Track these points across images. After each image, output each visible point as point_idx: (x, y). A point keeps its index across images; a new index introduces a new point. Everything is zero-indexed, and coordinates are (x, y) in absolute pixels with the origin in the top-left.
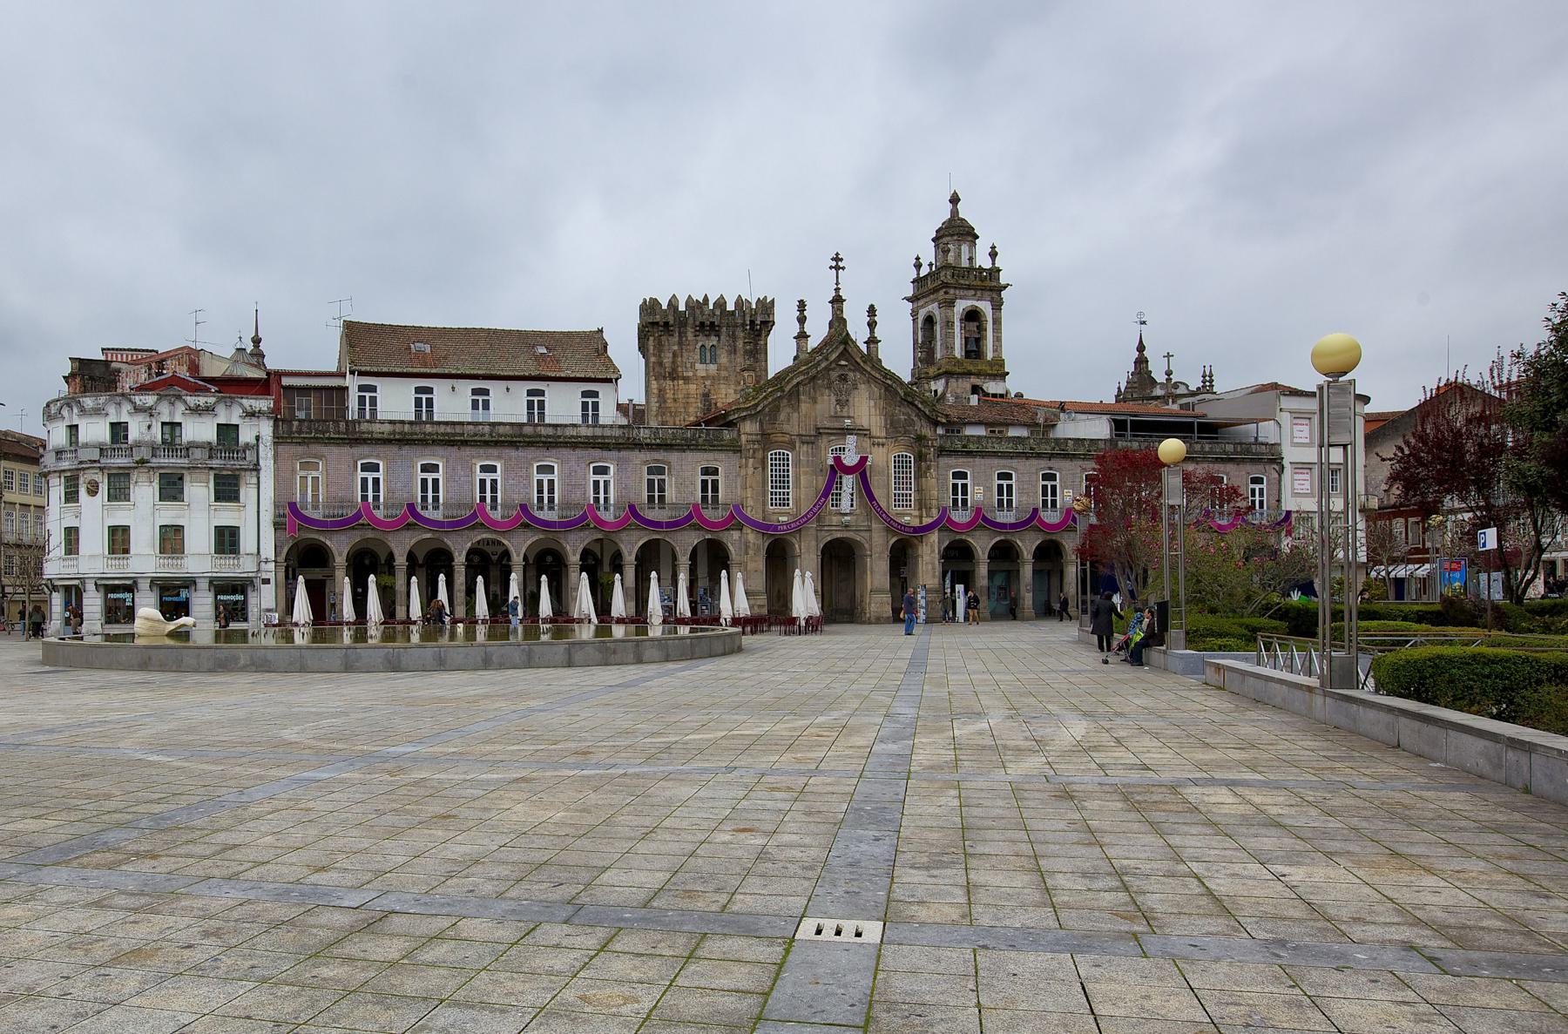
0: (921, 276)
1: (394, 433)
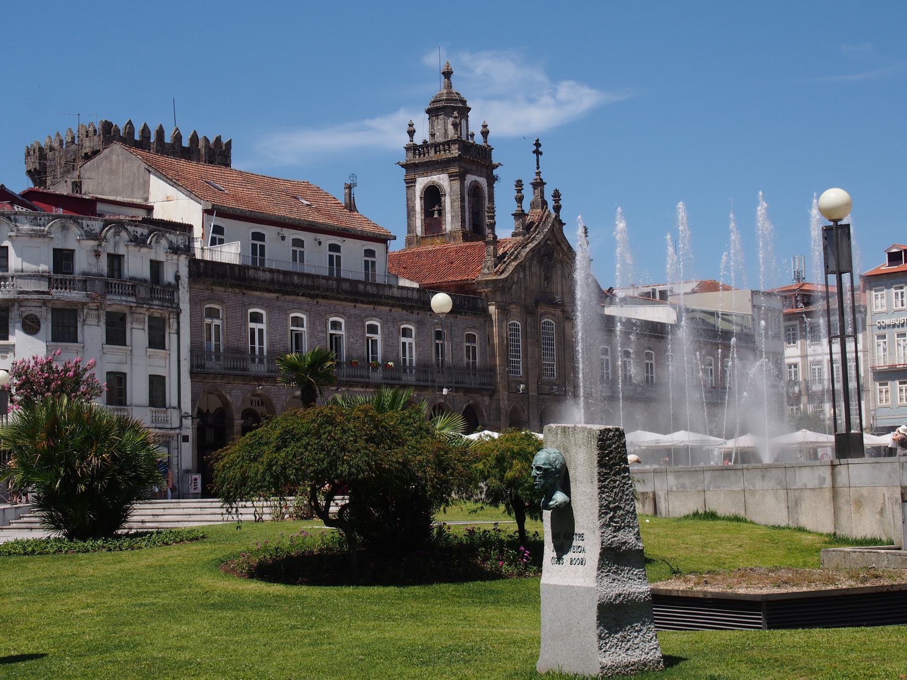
0: (418, 140)
1: (272, 281)
